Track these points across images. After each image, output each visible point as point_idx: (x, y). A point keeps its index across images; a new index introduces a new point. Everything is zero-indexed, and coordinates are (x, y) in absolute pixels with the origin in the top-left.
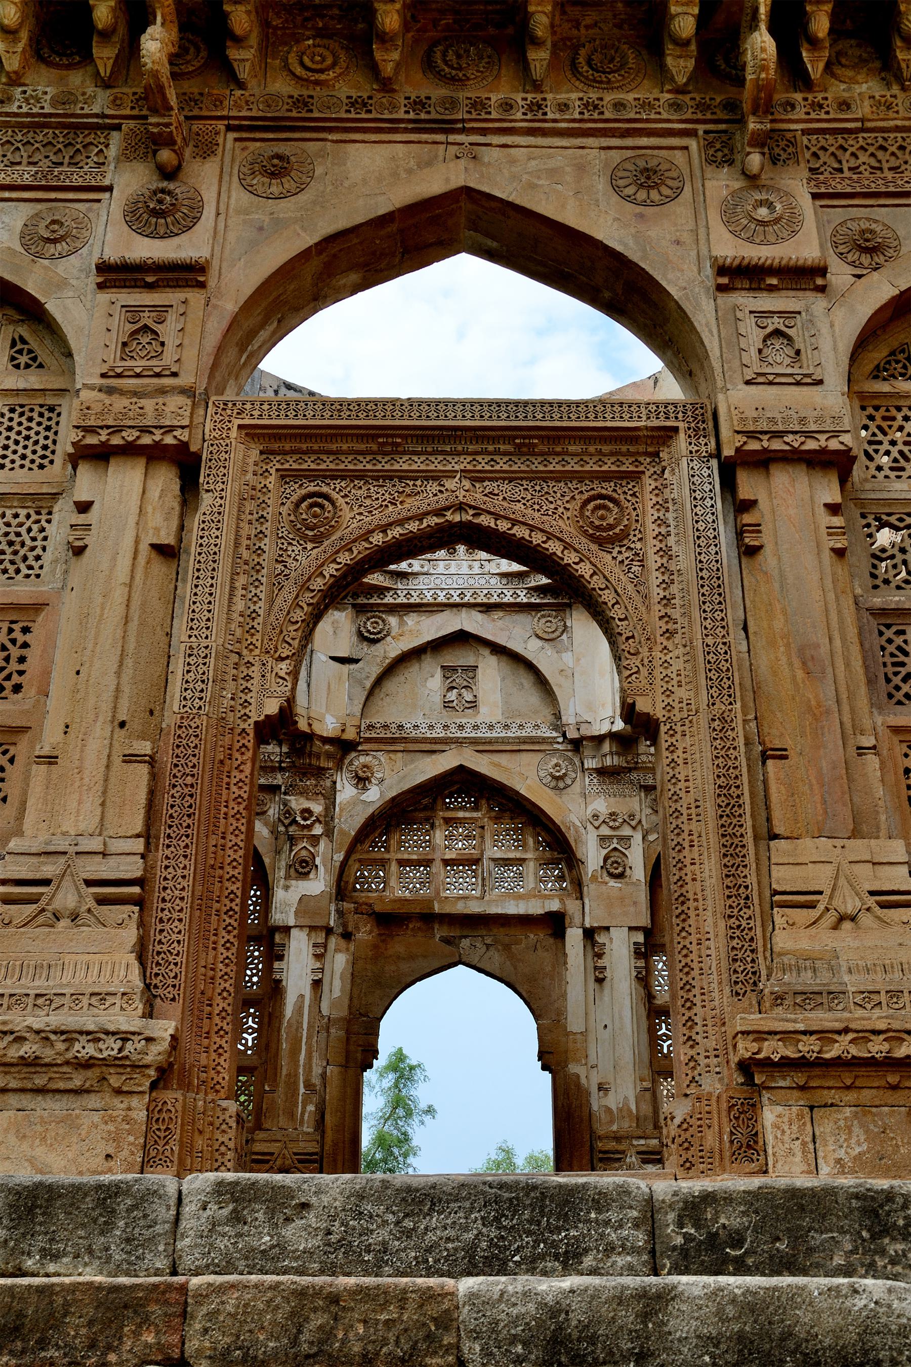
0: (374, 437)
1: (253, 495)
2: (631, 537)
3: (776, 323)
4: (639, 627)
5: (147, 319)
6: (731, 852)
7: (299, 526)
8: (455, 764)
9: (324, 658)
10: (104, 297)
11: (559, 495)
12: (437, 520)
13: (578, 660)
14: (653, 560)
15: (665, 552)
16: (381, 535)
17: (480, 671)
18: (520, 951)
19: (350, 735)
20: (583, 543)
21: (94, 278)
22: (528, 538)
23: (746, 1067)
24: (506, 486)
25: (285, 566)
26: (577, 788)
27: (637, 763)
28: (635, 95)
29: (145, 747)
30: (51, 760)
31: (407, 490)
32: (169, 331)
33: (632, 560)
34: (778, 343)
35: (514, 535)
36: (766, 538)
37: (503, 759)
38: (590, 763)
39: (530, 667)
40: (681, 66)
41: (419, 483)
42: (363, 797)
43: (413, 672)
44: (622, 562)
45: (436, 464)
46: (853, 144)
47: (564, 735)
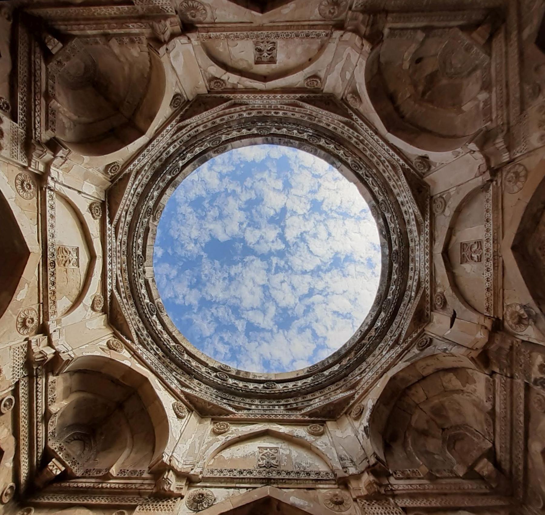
17: (464, 241)
43: (463, 281)
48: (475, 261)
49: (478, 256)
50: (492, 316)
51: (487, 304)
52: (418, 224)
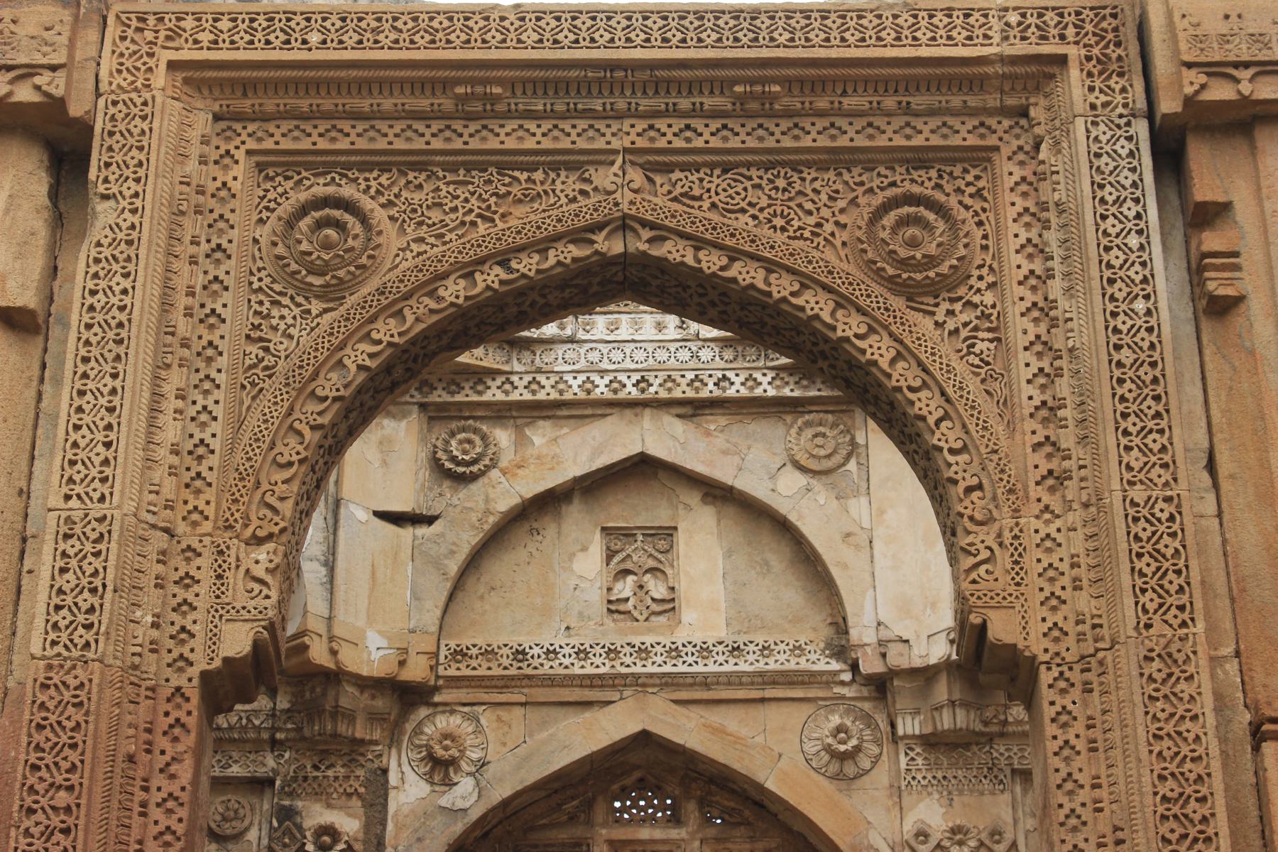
0: (446, 84)
1: (200, 204)
2: (973, 281)
4: (991, 466)
7: (294, 267)
8: (632, 728)
9: (362, 515)
11: (824, 197)
12: (576, 251)
13: (882, 512)
14: (1021, 329)
15: (1043, 311)
16: (462, 283)
17: (681, 537)
19: (416, 671)
20: (877, 296)
22: (761, 286)
24: (716, 180)
25: (266, 349)
26: (881, 776)
27: (1005, 722)
31: (515, 189)
33: (976, 329)
35: (734, 280)
36: (1251, 282)
37: (730, 719)
38: (909, 726)
39: (783, 527)
41: (538, 176)
42: (445, 801)
44: (956, 331)
45: (574, 137)
47: (854, 667)
48: (609, 589)
49: (627, 600)
50: (441, 671)
51: (474, 651)
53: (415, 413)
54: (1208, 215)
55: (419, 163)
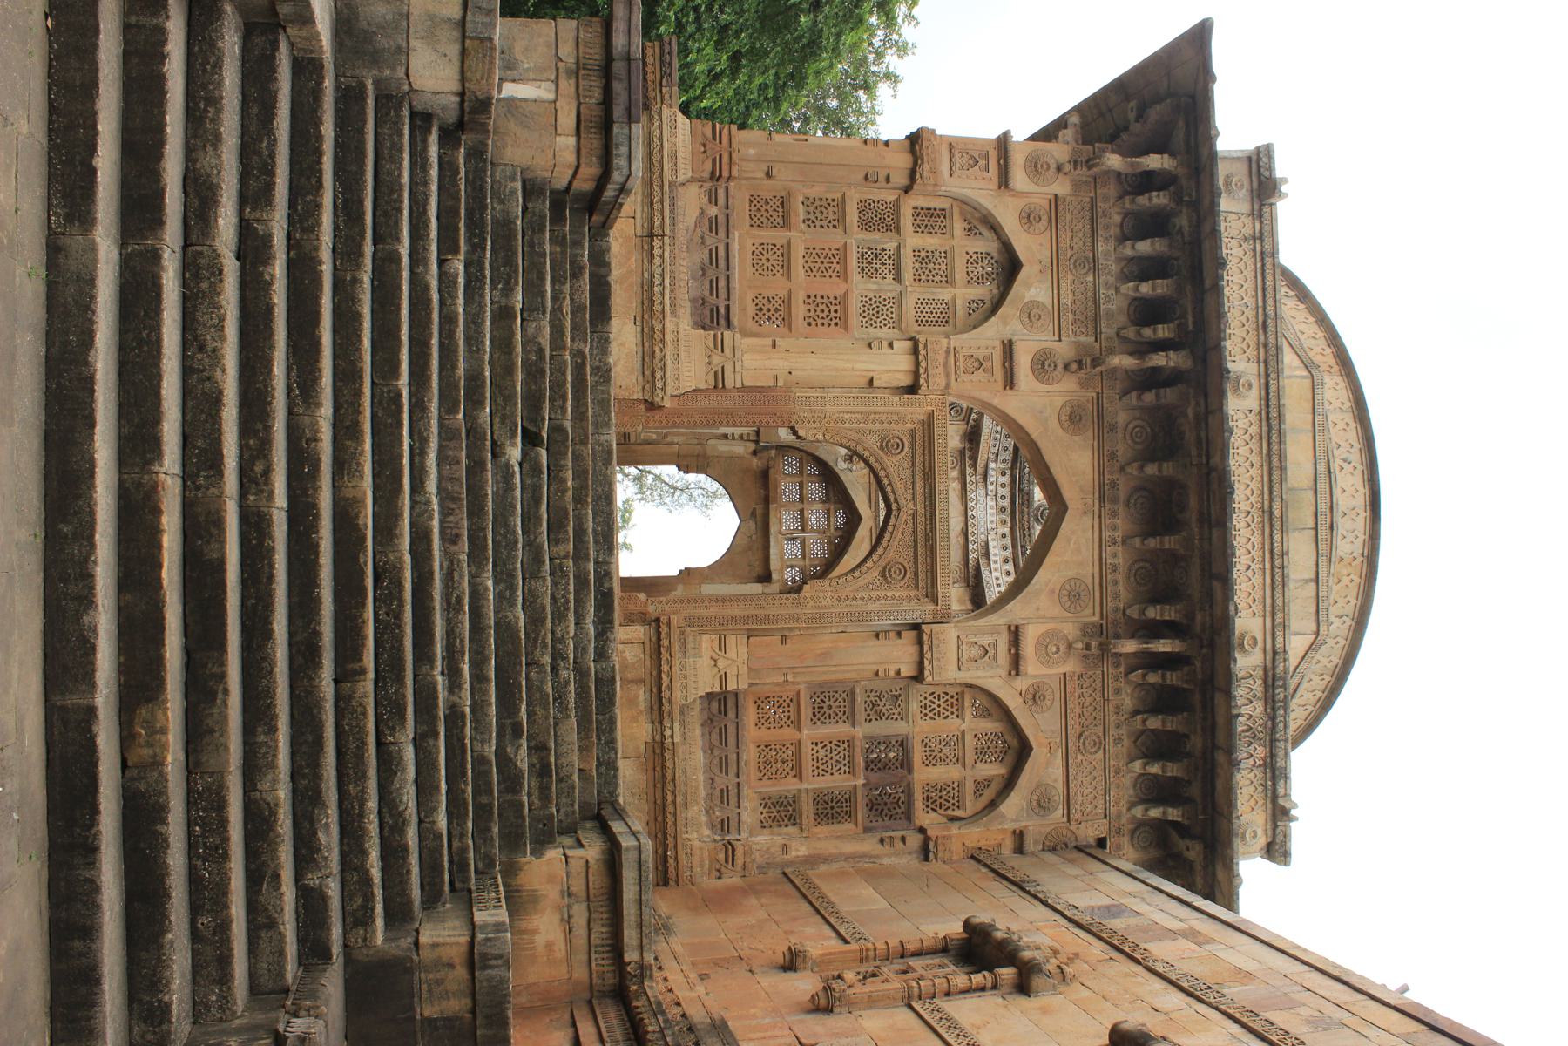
1: (901, 419)
3: (991, 651)
5: (986, 365)
6: (742, 619)
10: (998, 344)
14: (874, 594)
18: (750, 556)
20: (882, 564)
21: (1006, 337)
23: (657, 620)
28: (1123, 591)
29: (780, 384)
30: (774, 345)
32: (981, 376)
34: (981, 652)
36: (882, 641)
40: (1134, 613)
45: (920, 498)
46: (1098, 695)
52: (987, 555)
53: (960, 446)
54: (899, 634)
55: (914, 464)
